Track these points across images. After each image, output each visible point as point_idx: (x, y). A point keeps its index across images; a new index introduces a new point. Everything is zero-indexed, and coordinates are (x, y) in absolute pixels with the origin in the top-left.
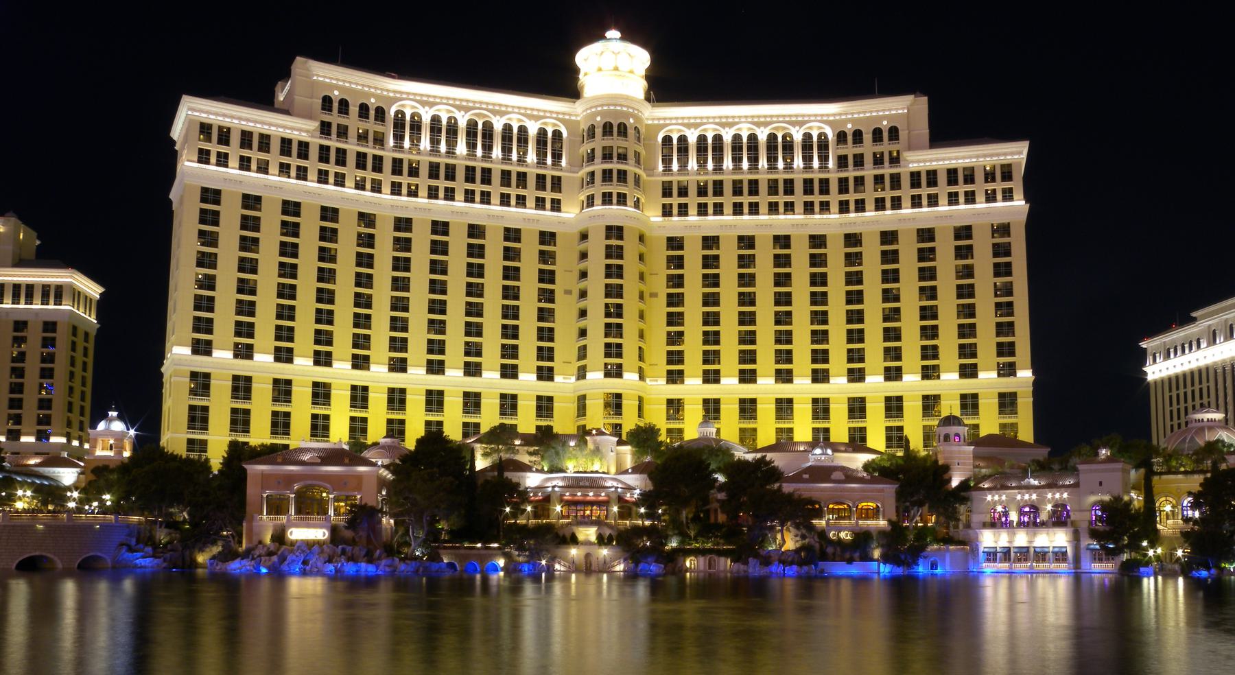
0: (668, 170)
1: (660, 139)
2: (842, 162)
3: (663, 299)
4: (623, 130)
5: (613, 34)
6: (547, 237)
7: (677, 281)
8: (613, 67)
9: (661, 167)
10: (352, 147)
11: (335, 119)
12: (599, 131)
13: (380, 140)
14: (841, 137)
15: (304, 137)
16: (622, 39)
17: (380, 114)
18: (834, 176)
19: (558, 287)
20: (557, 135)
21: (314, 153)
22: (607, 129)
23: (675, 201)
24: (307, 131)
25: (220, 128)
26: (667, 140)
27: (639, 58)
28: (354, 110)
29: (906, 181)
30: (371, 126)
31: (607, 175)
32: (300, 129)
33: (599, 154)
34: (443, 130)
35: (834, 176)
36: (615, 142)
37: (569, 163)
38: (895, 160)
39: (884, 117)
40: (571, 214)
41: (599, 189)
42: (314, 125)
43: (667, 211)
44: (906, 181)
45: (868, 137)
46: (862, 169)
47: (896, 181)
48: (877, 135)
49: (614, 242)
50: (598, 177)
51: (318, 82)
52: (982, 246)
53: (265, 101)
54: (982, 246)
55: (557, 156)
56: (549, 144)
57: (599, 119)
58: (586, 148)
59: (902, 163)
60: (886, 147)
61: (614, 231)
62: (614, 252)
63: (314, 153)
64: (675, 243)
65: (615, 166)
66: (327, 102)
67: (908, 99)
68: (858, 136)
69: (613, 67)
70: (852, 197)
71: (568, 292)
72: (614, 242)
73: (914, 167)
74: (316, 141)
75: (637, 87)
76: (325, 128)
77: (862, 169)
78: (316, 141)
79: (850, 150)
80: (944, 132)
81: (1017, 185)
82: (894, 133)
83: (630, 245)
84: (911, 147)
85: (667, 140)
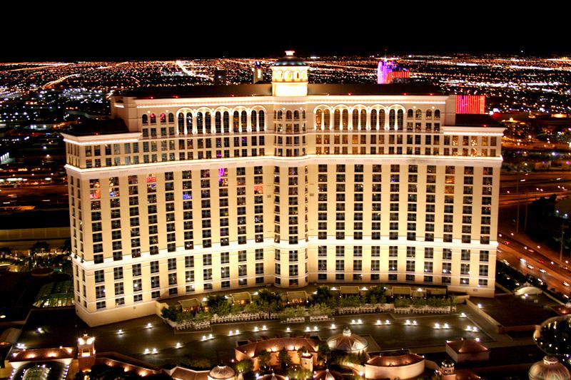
0: (319, 128)
1: (315, 112)
3: (317, 197)
7: (324, 188)
9: (315, 128)
11: (149, 127)
12: (284, 116)
13: (172, 133)
14: (410, 113)
15: (136, 141)
17: (171, 116)
18: (405, 134)
21: (141, 148)
22: (289, 115)
24: (137, 138)
29: (442, 140)
30: (167, 125)
34: (203, 121)
37: (268, 129)
44: (442, 140)
46: (422, 135)
47: (437, 138)
48: (429, 113)
51: (140, 109)
52: (478, 178)
54: (478, 178)
55: (262, 125)
57: (284, 109)
59: (441, 131)
60: (433, 121)
62: (292, 181)
63: (141, 148)
66: (145, 117)
71: (269, 196)
73: (446, 134)
78: (141, 143)
82: (437, 113)
84: (445, 125)
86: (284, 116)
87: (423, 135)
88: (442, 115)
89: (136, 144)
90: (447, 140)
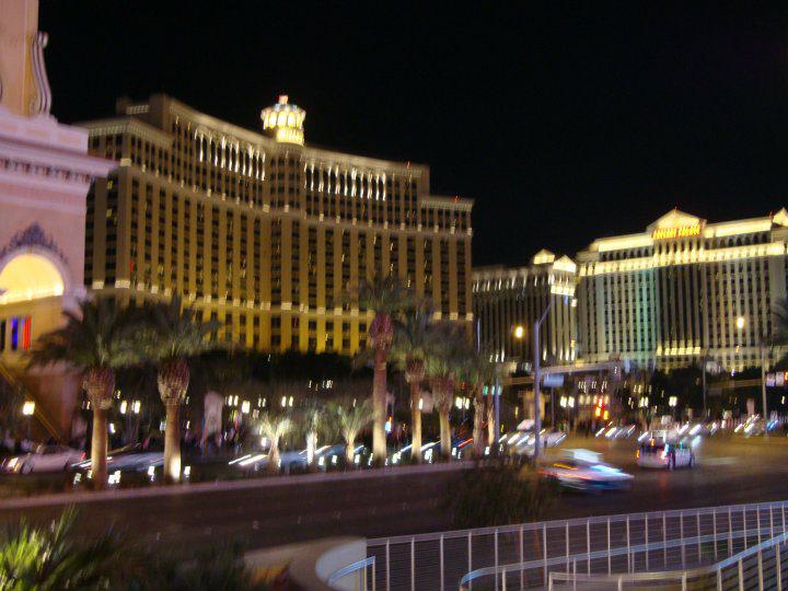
2: (389, 196)
8: (286, 121)
14: (389, 182)
16: (291, 102)
22: (292, 162)
32: (162, 141)
40: (266, 208)
56: (257, 164)
58: (276, 169)
62: (295, 235)
64: (312, 230)
66: (174, 125)
69: (286, 121)
75: (298, 138)
77: (399, 200)
80: (439, 188)
81: (468, 220)
82: (414, 185)
85: (309, 170)
88: (419, 186)
90: (424, 211)
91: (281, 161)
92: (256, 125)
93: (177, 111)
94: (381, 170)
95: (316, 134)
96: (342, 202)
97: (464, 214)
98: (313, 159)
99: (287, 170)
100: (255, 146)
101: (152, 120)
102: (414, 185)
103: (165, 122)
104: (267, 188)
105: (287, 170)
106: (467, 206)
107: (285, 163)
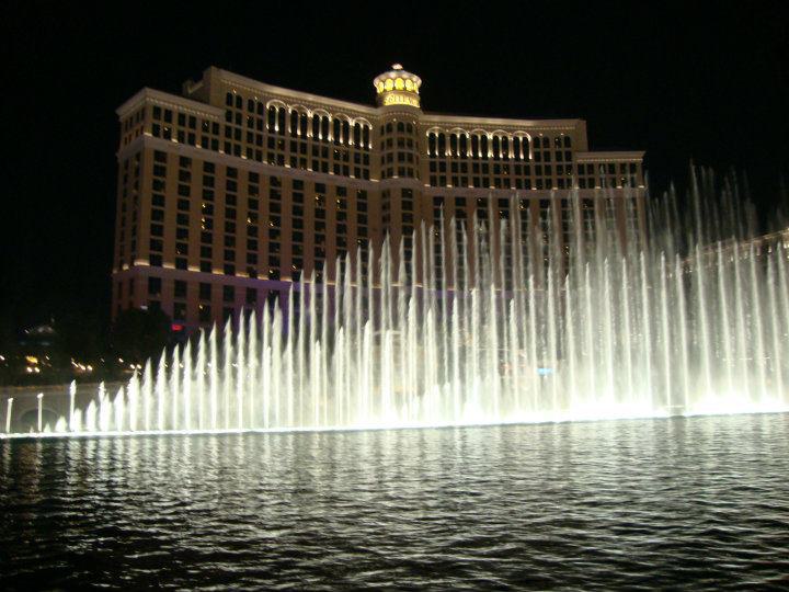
4: (410, 130)
5: (398, 67)
6: (363, 195)
8: (398, 88)
10: (244, 128)
12: (395, 128)
13: (260, 126)
14: (536, 140)
15: (216, 119)
16: (406, 68)
17: (261, 106)
18: (532, 165)
19: (369, 227)
20: (366, 127)
21: (222, 131)
22: (401, 127)
23: (438, 174)
25: (166, 111)
26: (432, 135)
27: (413, 83)
28: (245, 104)
29: (575, 169)
31: (401, 157)
33: (395, 142)
35: (532, 165)
36: (406, 136)
38: (569, 156)
39: (562, 131)
41: (396, 165)
42: (222, 112)
43: (433, 182)
45: (552, 143)
47: (569, 168)
49: (406, 199)
50: (395, 157)
53: (177, 90)
55: (366, 143)
58: (386, 137)
59: (574, 159)
61: (406, 192)
62: (407, 205)
63: (222, 131)
65: (406, 150)
66: (229, 96)
67: (576, 121)
68: (546, 141)
69: (398, 88)
70: (544, 177)
72: (406, 199)
74: (223, 123)
75: (415, 103)
76: (229, 117)
79: (542, 150)
80: (595, 144)
82: (567, 140)
83: (415, 200)
85: (432, 135)
86: (395, 128)
87: (553, 162)
89: (216, 126)
90: (581, 167)
91: (389, 128)
92: (373, 99)
93: (229, 81)
94: (524, 129)
95: (431, 100)
96: (476, 166)
97: (633, 167)
98: (435, 124)
99: (395, 136)
100: (356, 114)
101: (201, 98)
102: (567, 140)
103: (213, 95)
104: (375, 158)
105: (395, 136)
106: (636, 157)
107: (400, 127)
